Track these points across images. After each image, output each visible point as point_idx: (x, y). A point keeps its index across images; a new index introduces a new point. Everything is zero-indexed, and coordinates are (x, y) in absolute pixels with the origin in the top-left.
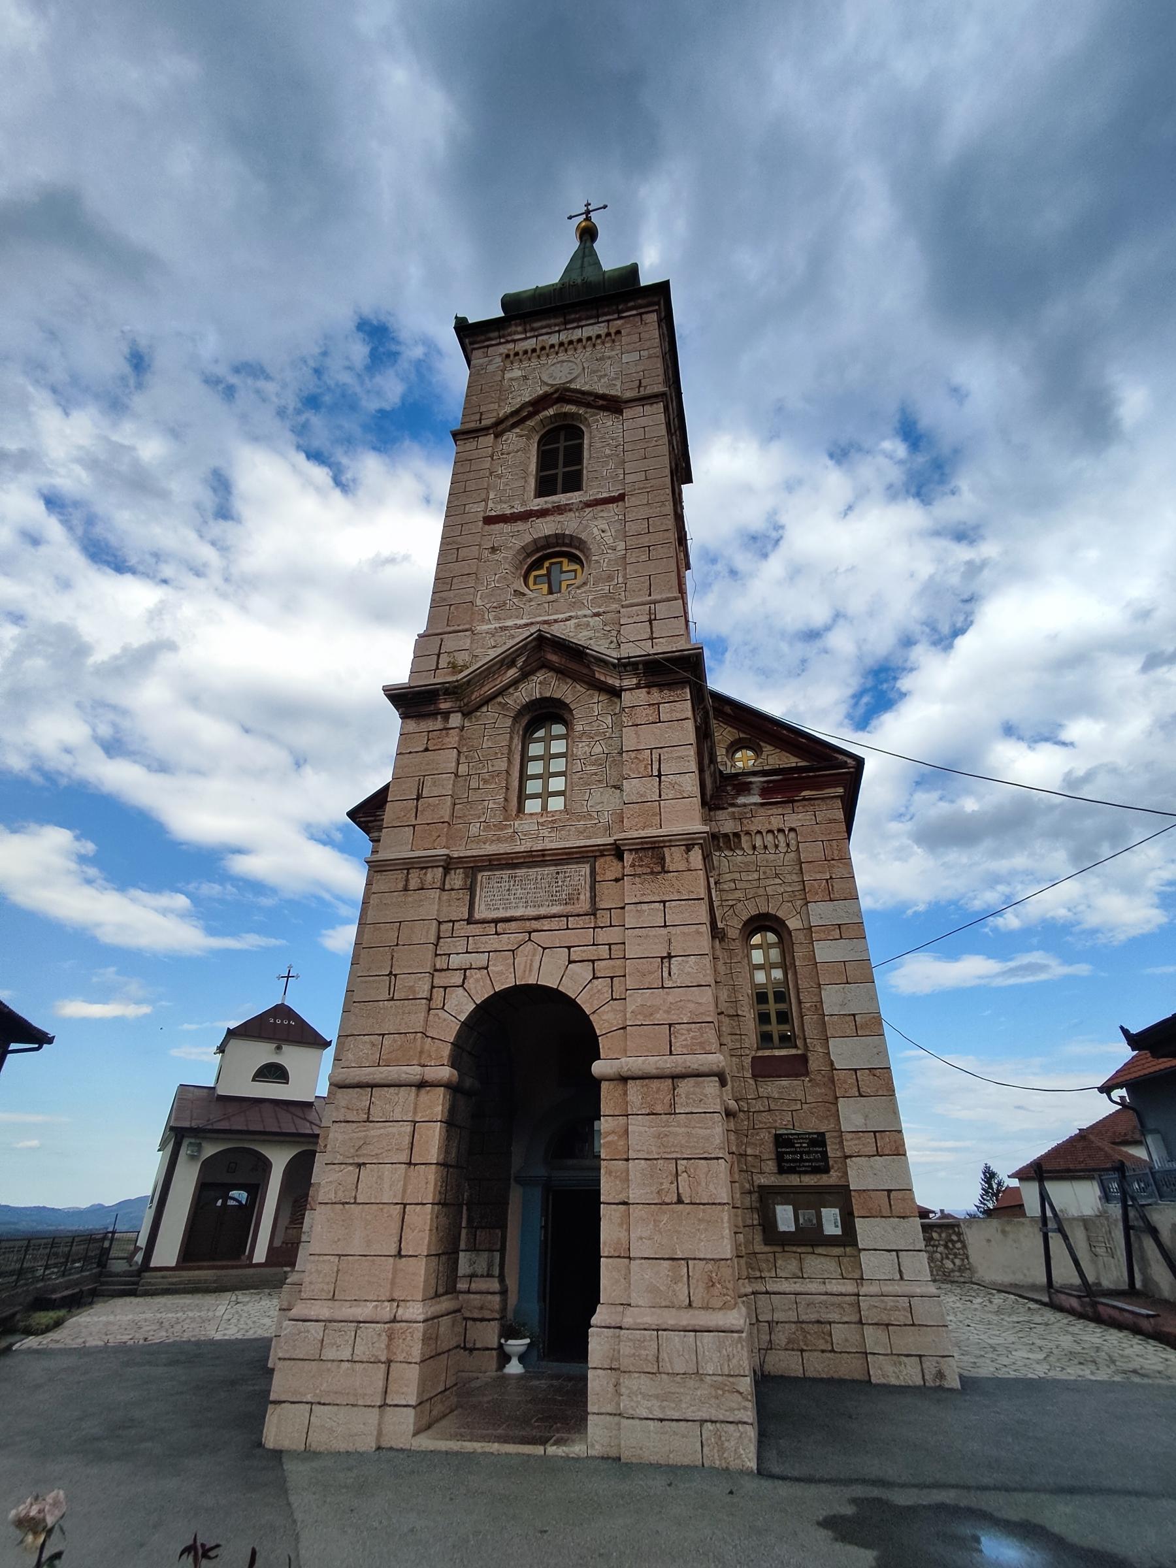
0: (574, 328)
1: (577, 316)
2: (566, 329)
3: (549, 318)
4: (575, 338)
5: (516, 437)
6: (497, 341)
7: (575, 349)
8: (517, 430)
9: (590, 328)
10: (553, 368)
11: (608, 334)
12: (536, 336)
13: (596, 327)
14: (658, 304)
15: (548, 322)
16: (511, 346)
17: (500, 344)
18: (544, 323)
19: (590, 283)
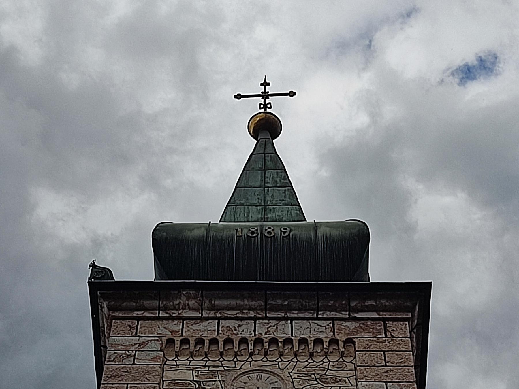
0: (279, 319)
1: (286, 303)
2: (266, 318)
3: (243, 298)
4: (280, 336)
6: (156, 313)
7: (281, 355)
9: (305, 324)
11: (334, 341)
12: (219, 319)
13: (313, 324)
14: (412, 312)
15: (239, 302)
16: (175, 325)
17: (159, 318)
18: (233, 302)
19: (295, 237)
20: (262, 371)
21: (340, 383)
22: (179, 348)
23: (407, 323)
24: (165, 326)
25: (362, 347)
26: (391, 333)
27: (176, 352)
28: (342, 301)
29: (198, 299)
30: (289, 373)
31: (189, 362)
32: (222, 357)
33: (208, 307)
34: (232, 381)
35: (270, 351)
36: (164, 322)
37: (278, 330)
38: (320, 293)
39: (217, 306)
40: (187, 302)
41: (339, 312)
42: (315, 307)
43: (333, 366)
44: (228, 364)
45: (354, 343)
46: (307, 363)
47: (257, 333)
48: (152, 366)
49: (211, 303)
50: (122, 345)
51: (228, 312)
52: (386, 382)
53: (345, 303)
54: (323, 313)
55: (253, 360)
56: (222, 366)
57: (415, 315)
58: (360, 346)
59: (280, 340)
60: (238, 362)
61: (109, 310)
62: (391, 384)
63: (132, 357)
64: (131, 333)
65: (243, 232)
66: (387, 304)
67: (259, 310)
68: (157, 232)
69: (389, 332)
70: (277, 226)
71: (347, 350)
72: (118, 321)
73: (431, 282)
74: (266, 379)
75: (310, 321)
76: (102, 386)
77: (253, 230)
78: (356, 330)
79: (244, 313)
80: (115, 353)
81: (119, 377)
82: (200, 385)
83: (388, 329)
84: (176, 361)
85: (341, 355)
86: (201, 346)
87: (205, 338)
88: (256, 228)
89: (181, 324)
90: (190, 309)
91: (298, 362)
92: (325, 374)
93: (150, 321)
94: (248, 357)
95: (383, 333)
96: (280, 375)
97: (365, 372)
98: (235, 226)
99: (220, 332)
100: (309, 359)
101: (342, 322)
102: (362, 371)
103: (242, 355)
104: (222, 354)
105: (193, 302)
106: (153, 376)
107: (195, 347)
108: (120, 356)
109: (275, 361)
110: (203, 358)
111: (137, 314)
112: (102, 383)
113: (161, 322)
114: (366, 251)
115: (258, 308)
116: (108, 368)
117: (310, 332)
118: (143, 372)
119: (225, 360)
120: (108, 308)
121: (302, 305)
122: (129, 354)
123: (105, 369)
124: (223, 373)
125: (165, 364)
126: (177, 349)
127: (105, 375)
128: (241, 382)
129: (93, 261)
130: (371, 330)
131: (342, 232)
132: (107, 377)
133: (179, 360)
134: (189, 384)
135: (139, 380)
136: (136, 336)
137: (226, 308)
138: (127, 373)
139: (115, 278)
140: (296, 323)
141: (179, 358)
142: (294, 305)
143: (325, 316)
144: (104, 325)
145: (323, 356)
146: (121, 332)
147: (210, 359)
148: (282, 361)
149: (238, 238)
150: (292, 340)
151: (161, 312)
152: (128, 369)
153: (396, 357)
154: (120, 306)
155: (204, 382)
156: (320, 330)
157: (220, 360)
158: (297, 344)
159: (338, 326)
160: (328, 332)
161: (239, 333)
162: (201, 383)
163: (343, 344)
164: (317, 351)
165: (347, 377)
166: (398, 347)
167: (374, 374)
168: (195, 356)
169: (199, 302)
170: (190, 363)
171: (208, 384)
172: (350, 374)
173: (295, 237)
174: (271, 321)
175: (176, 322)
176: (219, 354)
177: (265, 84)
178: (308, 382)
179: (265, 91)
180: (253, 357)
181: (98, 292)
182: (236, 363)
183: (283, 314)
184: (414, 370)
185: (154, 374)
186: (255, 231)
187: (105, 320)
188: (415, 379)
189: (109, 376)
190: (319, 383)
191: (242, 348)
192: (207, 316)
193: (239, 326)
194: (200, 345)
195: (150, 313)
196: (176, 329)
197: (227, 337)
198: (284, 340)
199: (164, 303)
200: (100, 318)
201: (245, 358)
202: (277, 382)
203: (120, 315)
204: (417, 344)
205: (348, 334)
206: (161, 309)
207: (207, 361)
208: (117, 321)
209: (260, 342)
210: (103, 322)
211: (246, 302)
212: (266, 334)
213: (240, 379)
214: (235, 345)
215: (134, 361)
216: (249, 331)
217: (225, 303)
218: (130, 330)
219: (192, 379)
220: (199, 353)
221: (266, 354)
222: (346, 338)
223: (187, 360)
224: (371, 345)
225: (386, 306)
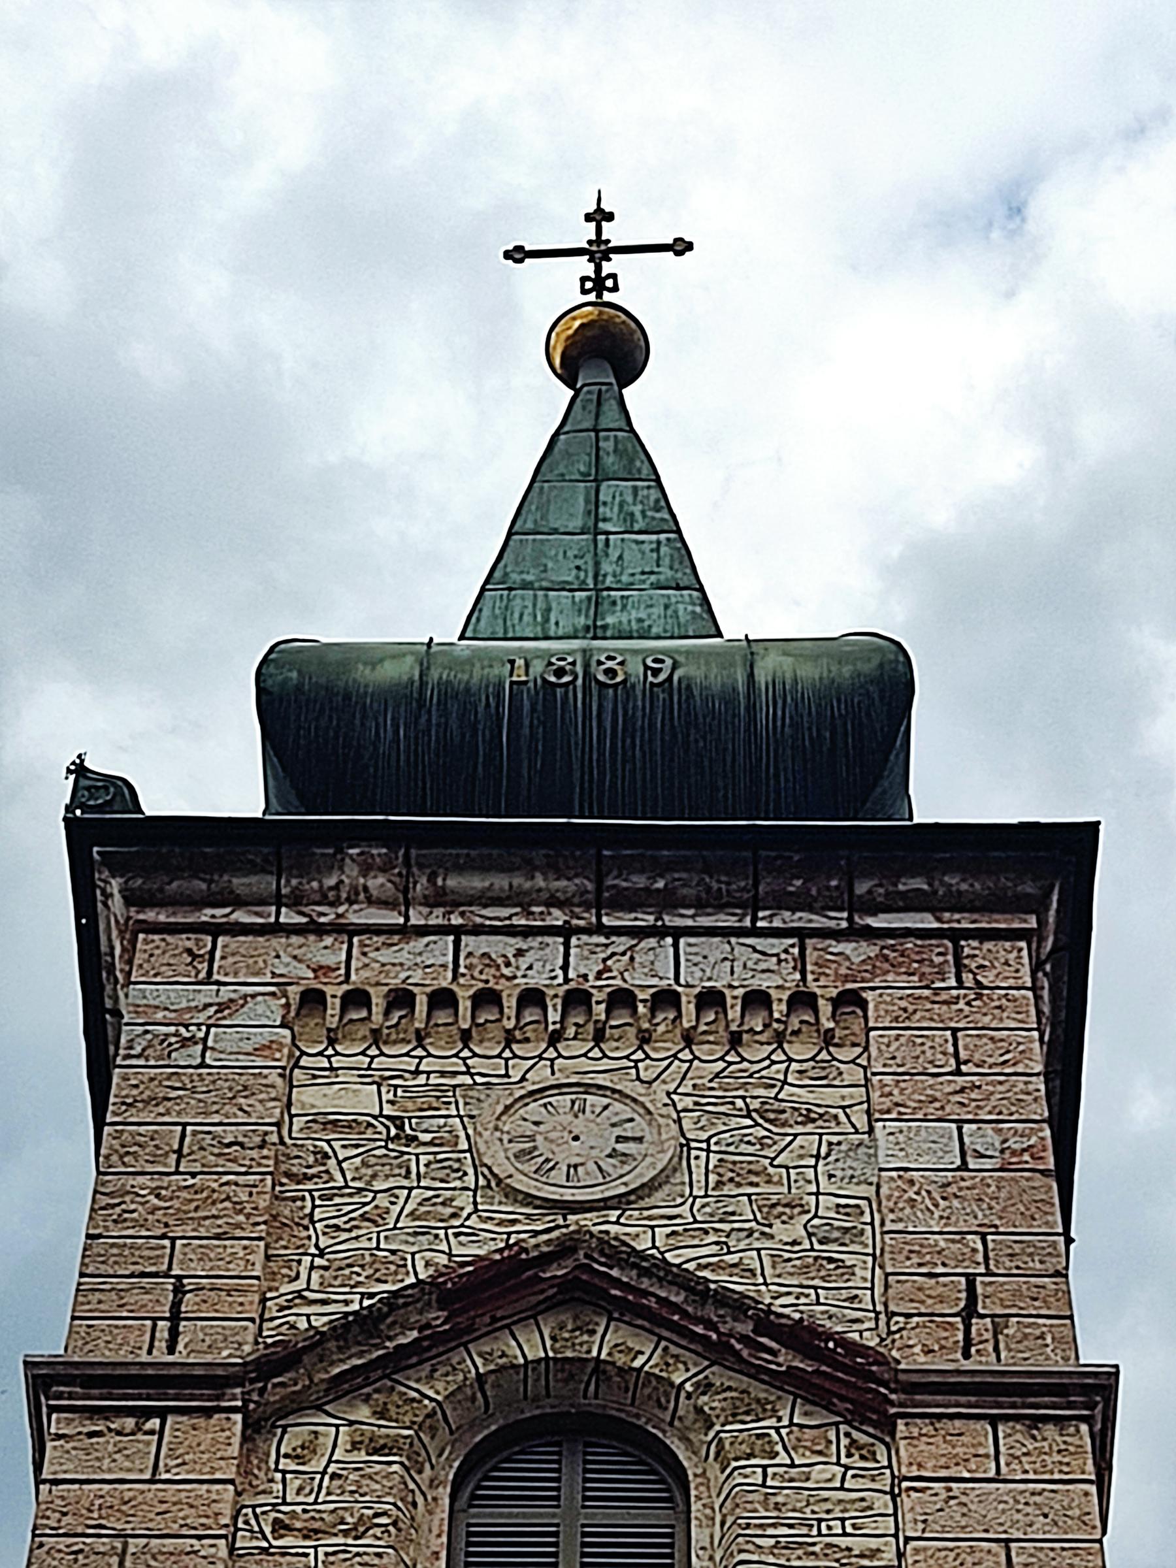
1: (660, 884)
2: (600, 929)
5: (355, 1446)
7: (644, 1039)
8: (363, 1413)
9: (716, 947)
10: (534, 1109)
11: (802, 1000)
13: (741, 949)
14: (1040, 910)
16: (330, 952)
17: (277, 929)
18: (500, 882)
19: (687, 686)
20: (589, 1088)
21: (820, 1123)
22: (337, 1018)
23: (1023, 944)
24: (296, 952)
25: (889, 1019)
26: (975, 974)
27: (329, 1030)
28: (829, 881)
29: (396, 871)
30: (668, 1094)
31: (368, 1060)
32: (466, 1046)
33: (425, 897)
34: (498, 1119)
35: (612, 1027)
36: (295, 940)
37: (636, 965)
38: (763, 853)
39: (453, 892)
40: (362, 880)
41: (821, 912)
42: (746, 896)
43: (799, 1072)
44: (487, 1067)
45: (863, 1004)
46: (721, 1065)
47: (572, 975)
48: (257, 1071)
49: (435, 884)
50: (166, 1009)
51: (484, 912)
52: (960, 1123)
53: (837, 887)
54: (771, 916)
55: (560, 1056)
56: (468, 1073)
57: (1047, 922)
58: (882, 1013)
59: (641, 996)
60: (517, 1061)
61: (128, 901)
62: (974, 1126)
63: (196, 1043)
64: (193, 974)
65: (531, 671)
66: (964, 887)
67: (579, 906)
68: (272, 669)
69: (971, 971)
70: (635, 652)
71: (842, 1025)
72: (156, 937)
73: (1099, 823)
74: (598, 1110)
75: (733, 940)
76: (106, 1129)
77: (562, 663)
78: (869, 968)
79: (533, 913)
80: (147, 1032)
81: (157, 1105)
82: (401, 1128)
83: (966, 962)
84: (329, 1057)
85: (825, 1041)
86: (403, 1013)
87: (416, 990)
88: (570, 659)
89: (345, 946)
90: (370, 901)
91: (696, 1062)
92: (776, 1098)
93: (250, 938)
94: (544, 1046)
95: (952, 976)
96: (641, 1099)
97: (896, 1092)
98: (508, 651)
99: (462, 970)
100: (727, 1053)
101: (828, 942)
102: (887, 1089)
103: (527, 1040)
104: (466, 1036)
105: (381, 880)
106: (261, 1101)
107: (387, 1014)
108: (163, 1041)
109: (627, 1057)
110: (410, 1047)
111: (213, 916)
112: (108, 1120)
113: (283, 940)
114: (903, 729)
115: (576, 900)
116: (125, 1078)
117: (732, 973)
118: (230, 1089)
119: (475, 1055)
120: (124, 897)
121: (709, 889)
122: (188, 1035)
123: (115, 1080)
124: (470, 1093)
125: (296, 1065)
126: (333, 1023)
127: (116, 1096)
128: (525, 1120)
129: (79, 756)
130: (916, 965)
131: (830, 671)
132: (123, 1103)
133: (337, 1054)
134: (370, 1125)
135: (217, 1112)
136: (208, 981)
137: (480, 898)
138: (181, 1093)
139: (144, 807)
140: (690, 945)
141: (338, 1048)
142: (685, 891)
143: (777, 923)
144: (112, 948)
145: (769, 1044)
146: (164, 969)
147: (433, 1051)
148: (648, 1057)
149: (515, 687)
150: (677, 995)
151: (283, 910)
152: (187, 1081)
153: (991, 1046)
154: (161, 890)
155: (414, 1121)
156: (763, 966)
157: (462, 1055)
158: (692, 1007)
159: (816, 953)
160: (784, 972)
161: (519, 974)
162: (403, 1123)
163: (830, 1008)
164: (751, 1030)
165: (843, 1108)
166: (994, 1018)
167: (923, 1098)
168: (385, 1043)
169: (397, 880)
170: (371, 1063)
171: (424, 1126)
172: (852, 1097)
173: (689, 687)
174: (614, 939)
175: (328, 940)
176: (457, 1037)
177: (600, 216)
178: (726, 1119)
179: (599, 240)
180: (559, 1046)
181: (95, 849)
182: (511, 1063)
183: (651, 918)
184: (1042, 1087)
185: (263, 1096)
186: (568, 668)
187: (115, 933)
188: (1046, 1114)
189: (129, 1100)
190: (757, 1124)
191: (528, 1019)
192: (422, 922)
193: (520, 953)
194: (400, 1009)
195: (250, 913)
196: (329, 959)
197: (481, 985)
198: (653, 995)
199: (294, 882)
200: (102, 927)
201: (536, 1048)
202: (631, 1120)
203: (162, 918)
204: (1054, 1010)
205: (846, 979)
206: (284, 900)
207: (421, 1058)
208: (151, 937)
209: (581, 1003)
210: (110, 940)
211: (540, 882)
212: (599, 976)
213: (521, 1111)
214: (506, 1010)
215: (203, 1056)
216: (548, 967)
217: (477, 883)
218: (191, 963)
219: (376, 1112)
220: (398, 1033)
221: (599, 1037)
222: (840, 989)
223: (363, 1053)
224: (915, 1011)
225: (959, 892)
